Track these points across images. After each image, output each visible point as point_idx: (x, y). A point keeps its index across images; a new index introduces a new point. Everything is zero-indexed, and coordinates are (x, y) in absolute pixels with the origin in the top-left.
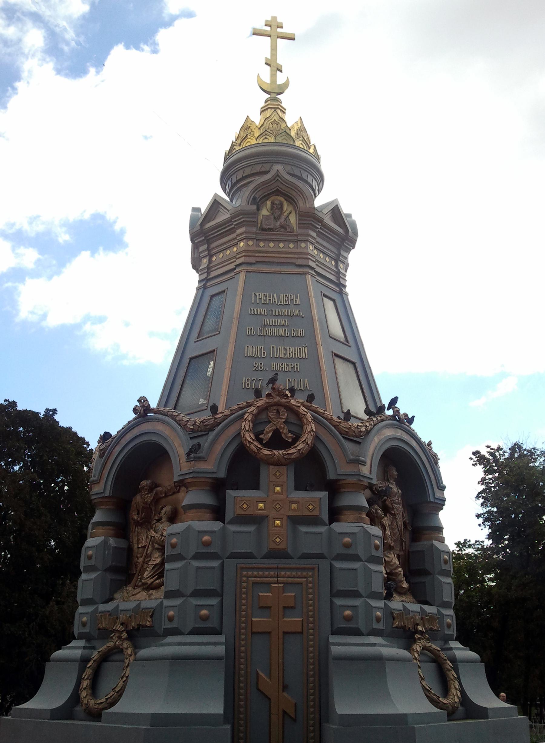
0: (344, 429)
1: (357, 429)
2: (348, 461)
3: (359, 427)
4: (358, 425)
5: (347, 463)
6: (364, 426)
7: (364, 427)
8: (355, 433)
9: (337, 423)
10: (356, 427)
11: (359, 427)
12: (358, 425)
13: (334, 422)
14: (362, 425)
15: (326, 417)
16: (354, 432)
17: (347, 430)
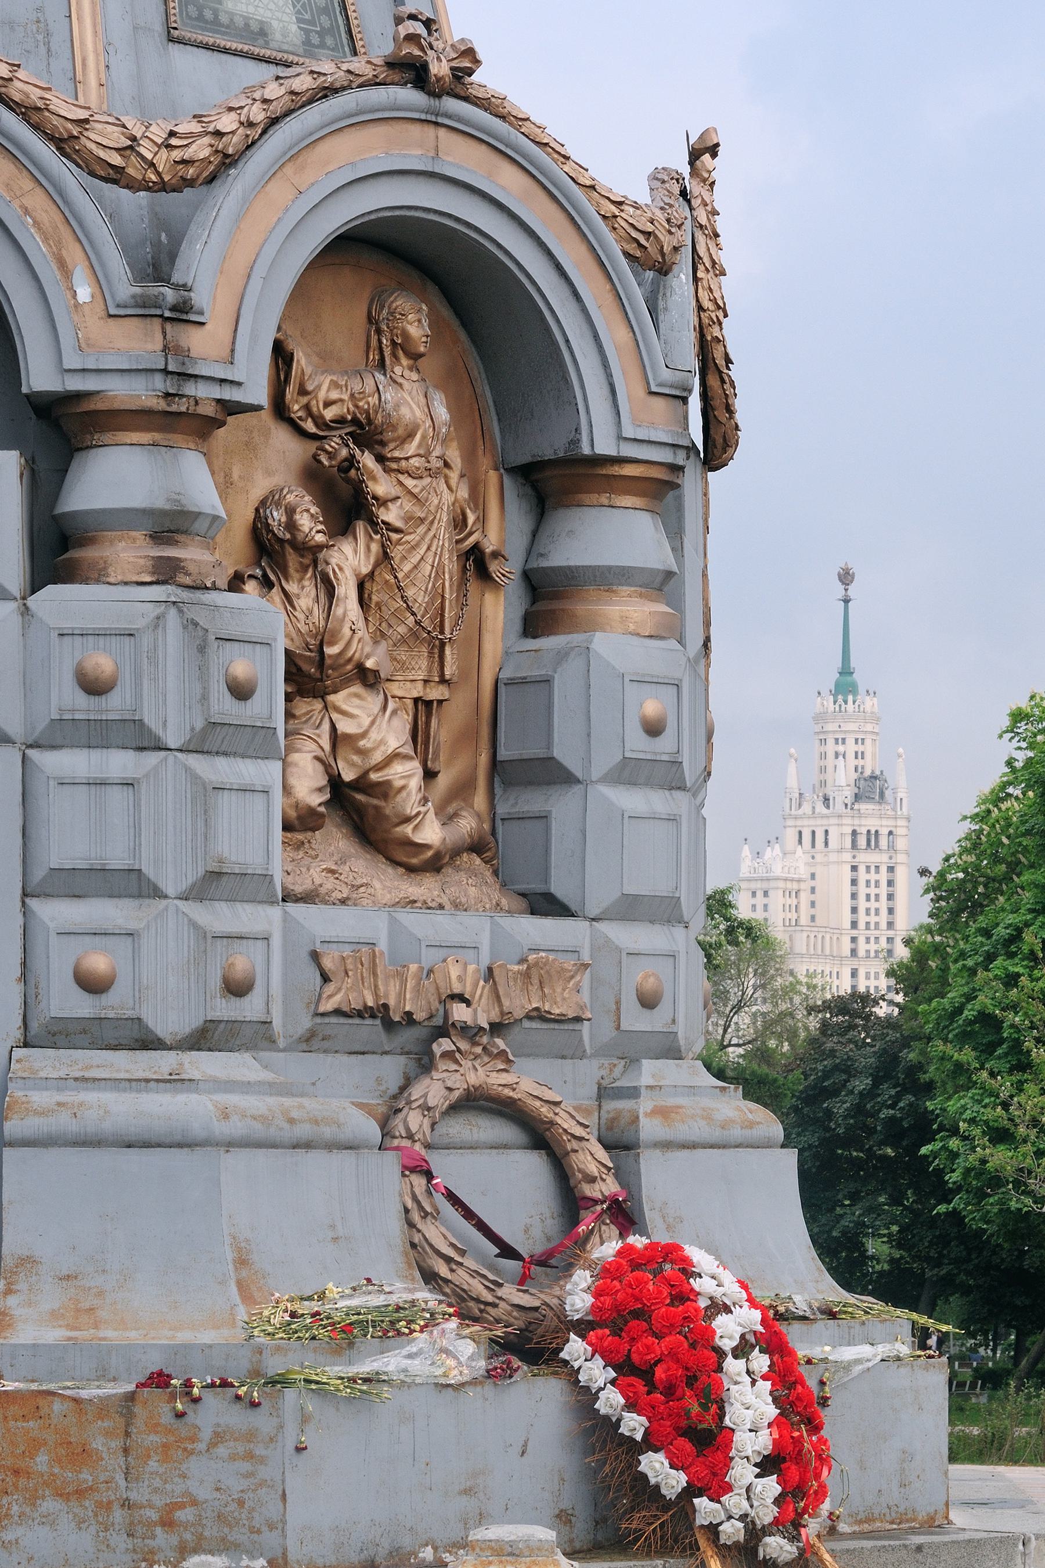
0: (102, 154)
1: (164, 153)
2: (112, 312)
3: (174, 142)
4: (172, 134)
5: (110, 316)
6: (207, 133)
7: (207, 140)
8: (159, 174)
9: (69, 126)
10: (159, 141)
11: (174, 142)
12: (172, 134)
13: (55, 121)
14: (195, 127)
15: (17, 97)
16: (152, 165)
17: (116, 160)
